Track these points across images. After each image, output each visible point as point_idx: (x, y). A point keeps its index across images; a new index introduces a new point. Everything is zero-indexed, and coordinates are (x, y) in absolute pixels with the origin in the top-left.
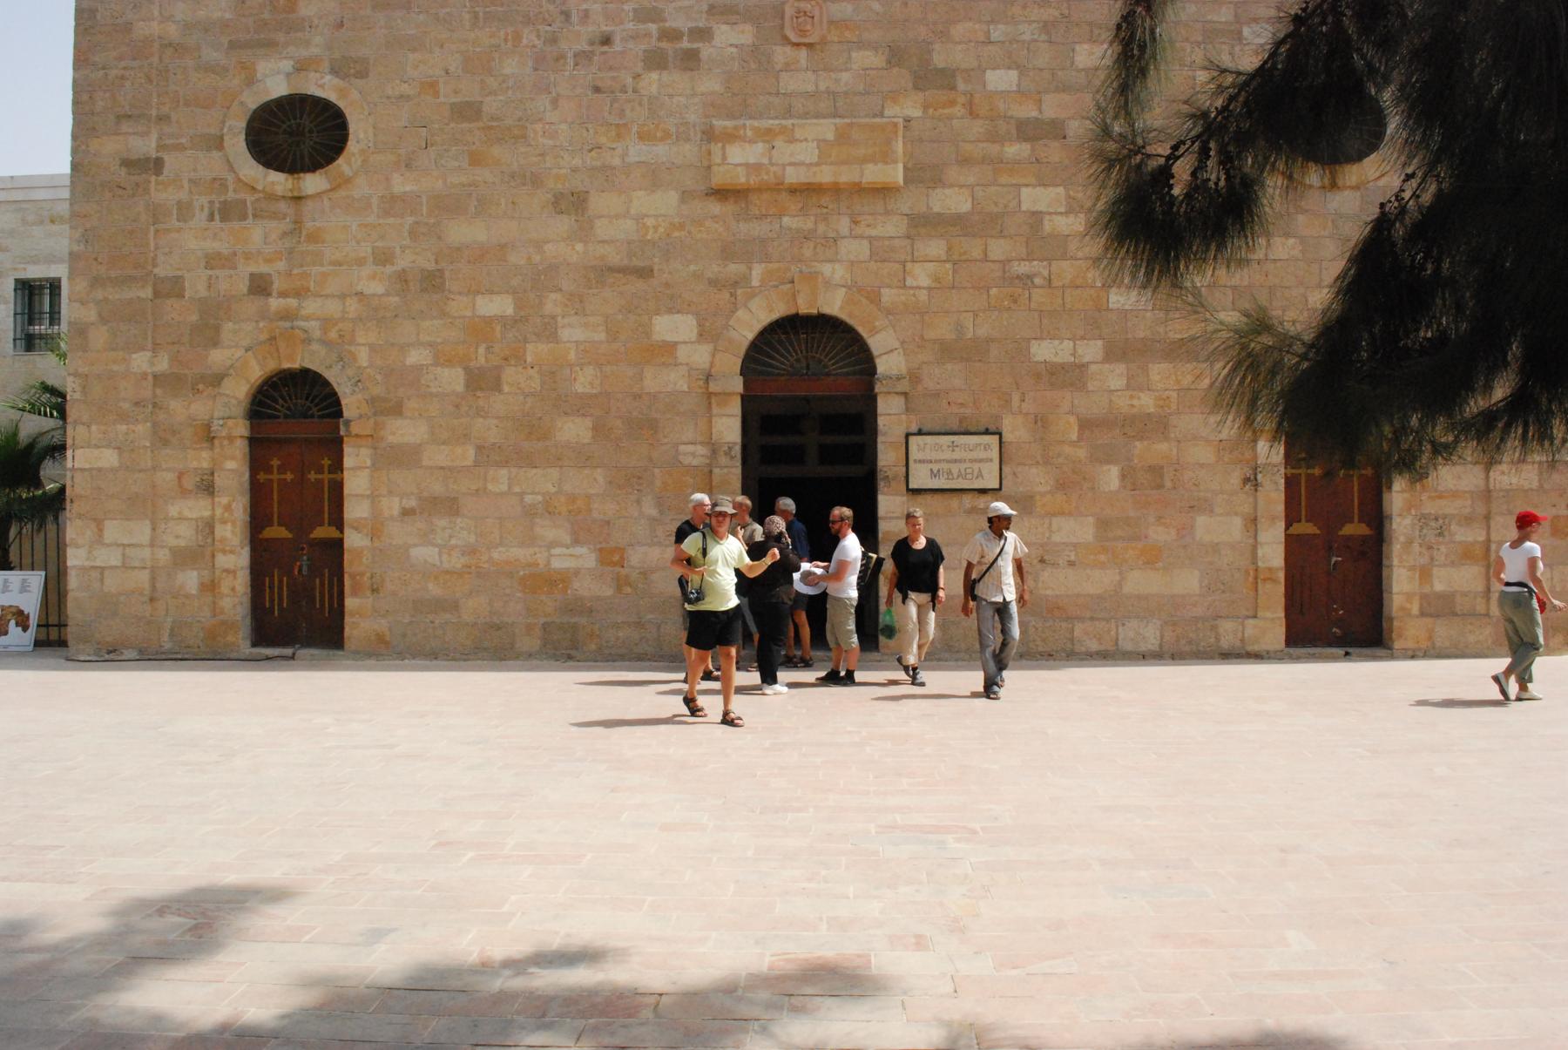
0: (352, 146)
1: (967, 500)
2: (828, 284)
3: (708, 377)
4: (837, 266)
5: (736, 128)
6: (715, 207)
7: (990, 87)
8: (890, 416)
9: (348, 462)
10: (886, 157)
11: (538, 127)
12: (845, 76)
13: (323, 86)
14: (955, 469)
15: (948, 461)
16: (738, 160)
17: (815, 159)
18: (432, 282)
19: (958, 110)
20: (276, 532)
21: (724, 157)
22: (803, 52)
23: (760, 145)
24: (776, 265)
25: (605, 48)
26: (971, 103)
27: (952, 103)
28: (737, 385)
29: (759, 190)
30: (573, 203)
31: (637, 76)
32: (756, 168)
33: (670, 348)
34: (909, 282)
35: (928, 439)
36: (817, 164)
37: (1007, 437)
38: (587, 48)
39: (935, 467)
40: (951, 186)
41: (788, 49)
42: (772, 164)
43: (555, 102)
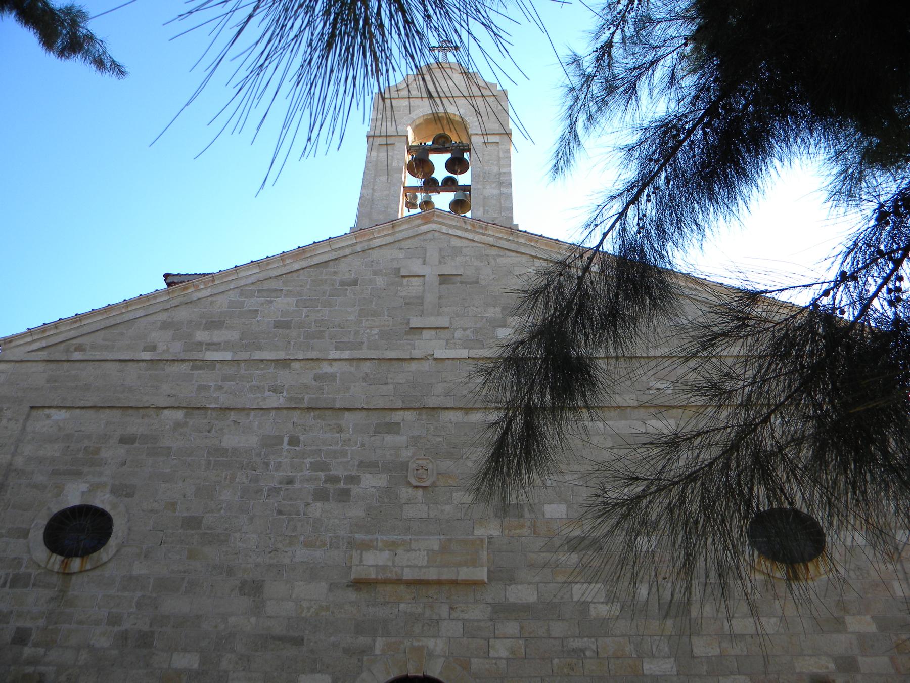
0: (113, 542)
2: (431, 655)
4: (439, 641)
5: (371, 541)
6: (352, 595)
7: (548, 516)
10: (474, 562)
11: (237, 535)
12: (447, 508)
13: (102, 501)
16: (371, 562)
17: (425, 563)
18: (145, 640)
19: (526, 531)
21: (361, 561)
22: (420, 492)
23: (387, 552)
24: (394, 639)
25: (289, 486)
26: (534, 526)
27: (522, 526)
29: (386, 582)
32: (384, 568)
34: (493, 653)
36: (426, 567)
38: (277, 485)
40: (522, 583)
41: (410, 490)
42: (395, 566)
43: (251, 519)
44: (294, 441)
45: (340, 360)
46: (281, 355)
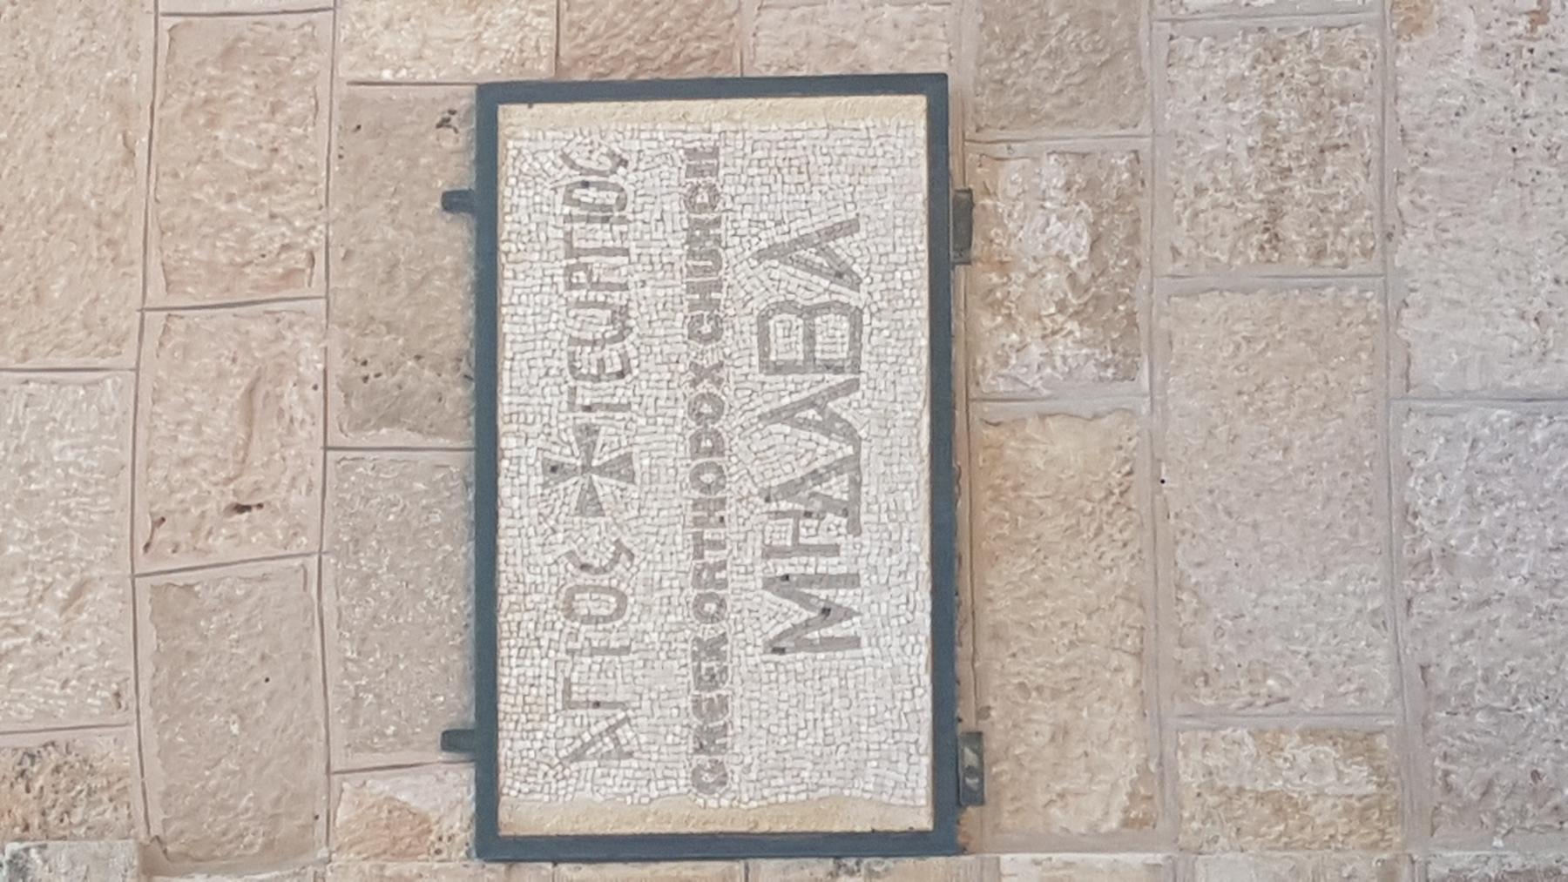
1: (1030, 353)
14: (766, 455)
15: (709, 505)
35: (516, 672)
37: (515, 40)
39: (758, 613)
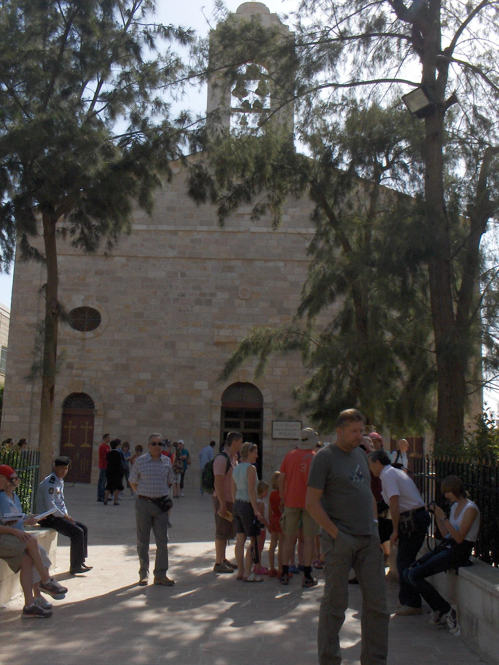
3: (211, 402)
6: (215, 348)
8: (267, 414)
9: (96, 423)
13: (93, 305)
20: (69, 445)
22: (244, 301)
25: (183, 298)
28: (220, 404)
30: (171, 345)
31: (192, 307)
33: (199, 392)
41: (239, 300)
44: (183, 275)
45: (203, 231)
46: (172, 228)
